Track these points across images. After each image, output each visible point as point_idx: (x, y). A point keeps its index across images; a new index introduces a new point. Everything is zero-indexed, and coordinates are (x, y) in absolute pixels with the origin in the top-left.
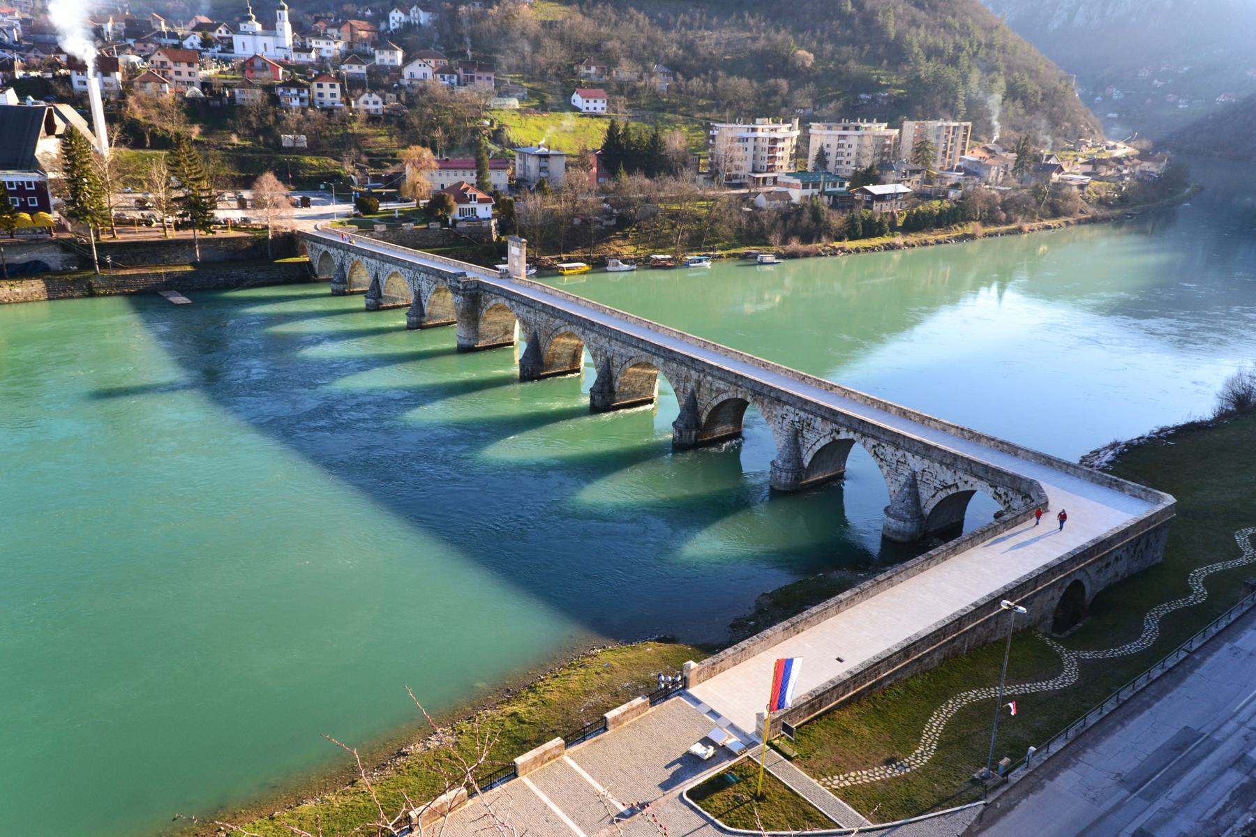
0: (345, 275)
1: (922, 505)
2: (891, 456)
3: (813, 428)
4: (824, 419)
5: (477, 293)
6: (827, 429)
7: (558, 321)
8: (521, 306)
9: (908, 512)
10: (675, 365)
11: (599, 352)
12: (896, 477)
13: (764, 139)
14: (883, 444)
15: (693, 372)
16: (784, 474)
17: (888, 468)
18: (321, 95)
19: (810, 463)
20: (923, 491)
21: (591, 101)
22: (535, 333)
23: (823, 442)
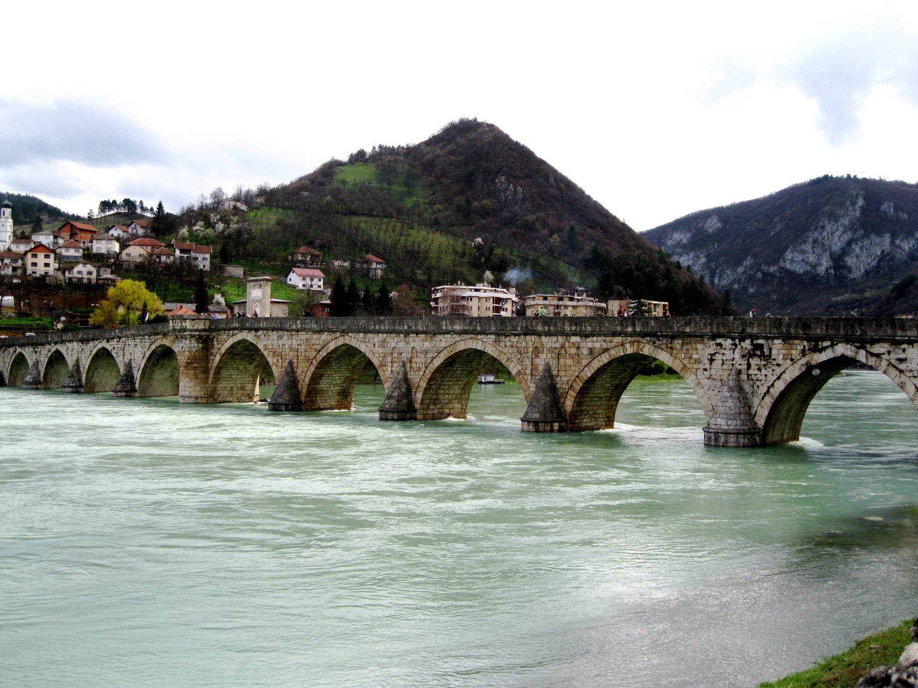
0: (39, 374)
5: (208, 336)
7: (325, 336)
8: (270, 333)
11: (389, 359)
13: (487, 299)
18: (34, 264)
19: (768, 418)
22: (291, 363)
23: (789, 377)
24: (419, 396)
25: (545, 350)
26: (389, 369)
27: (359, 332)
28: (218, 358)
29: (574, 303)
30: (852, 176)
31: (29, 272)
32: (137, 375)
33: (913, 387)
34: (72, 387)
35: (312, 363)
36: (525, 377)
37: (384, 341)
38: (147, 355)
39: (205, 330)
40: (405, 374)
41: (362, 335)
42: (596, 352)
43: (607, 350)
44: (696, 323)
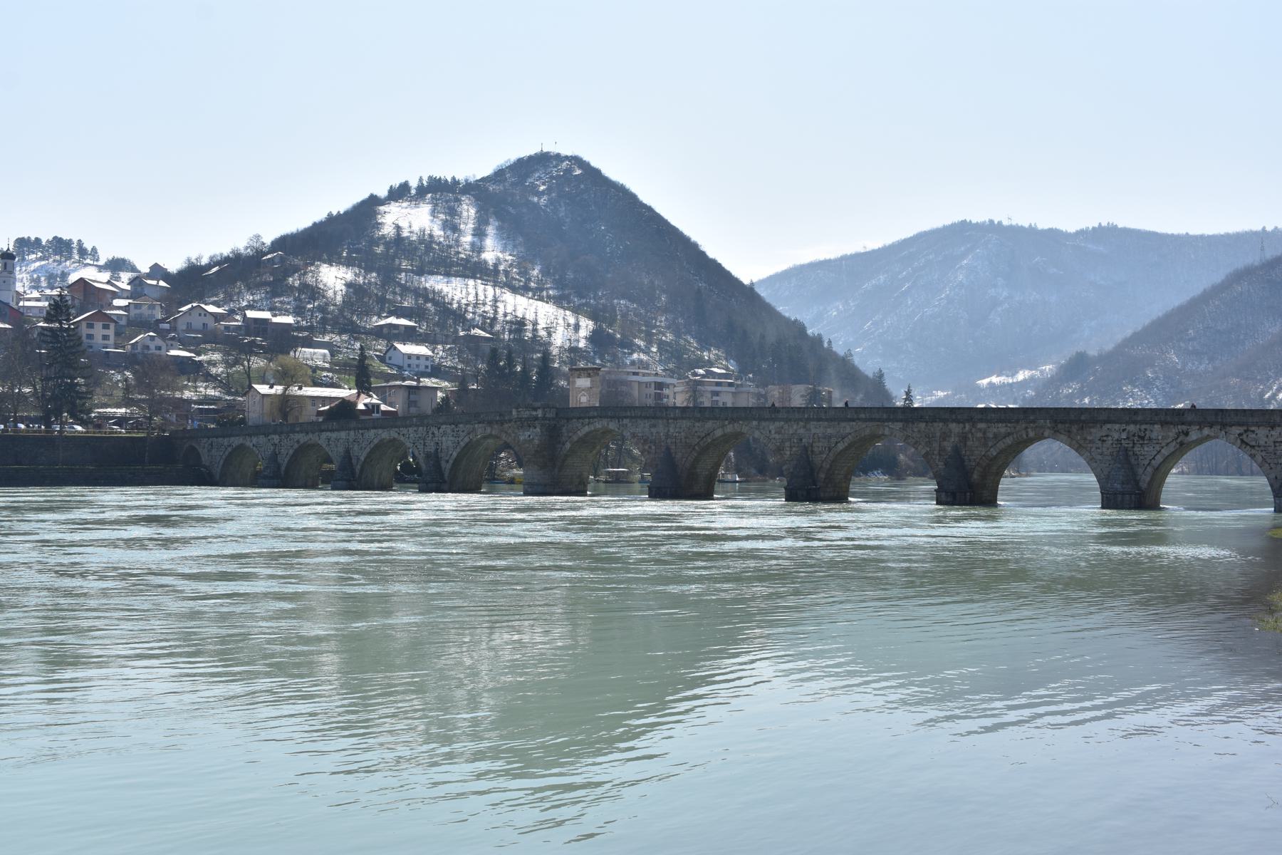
2: (1265, 439)
3: (1150, 439)
4: (1164, 424)
5: (555, 425)
6: (1170, 434)
7: (709, 424)
8: (639, 421)
10: (923, 425)
11: (787, 444)
12: (1276, 461)
13: (647, 385)
14: (1253, 428)
15: (953, 426)
16: (1127, 497)
17: (1264, 454)
18: (90, 337)
24: (822, 476)
25: (953, 435)
26: (788, 453)
28: (568, 445)
29: (733, 389)
30: (996, 222)
33: (1261, 457)
35: (694, 449)
36: (934, 457)
38: (462, 444)
39: (553, 419)
40: (808, 457)
41: (755, 423)
43: (1009, 434)
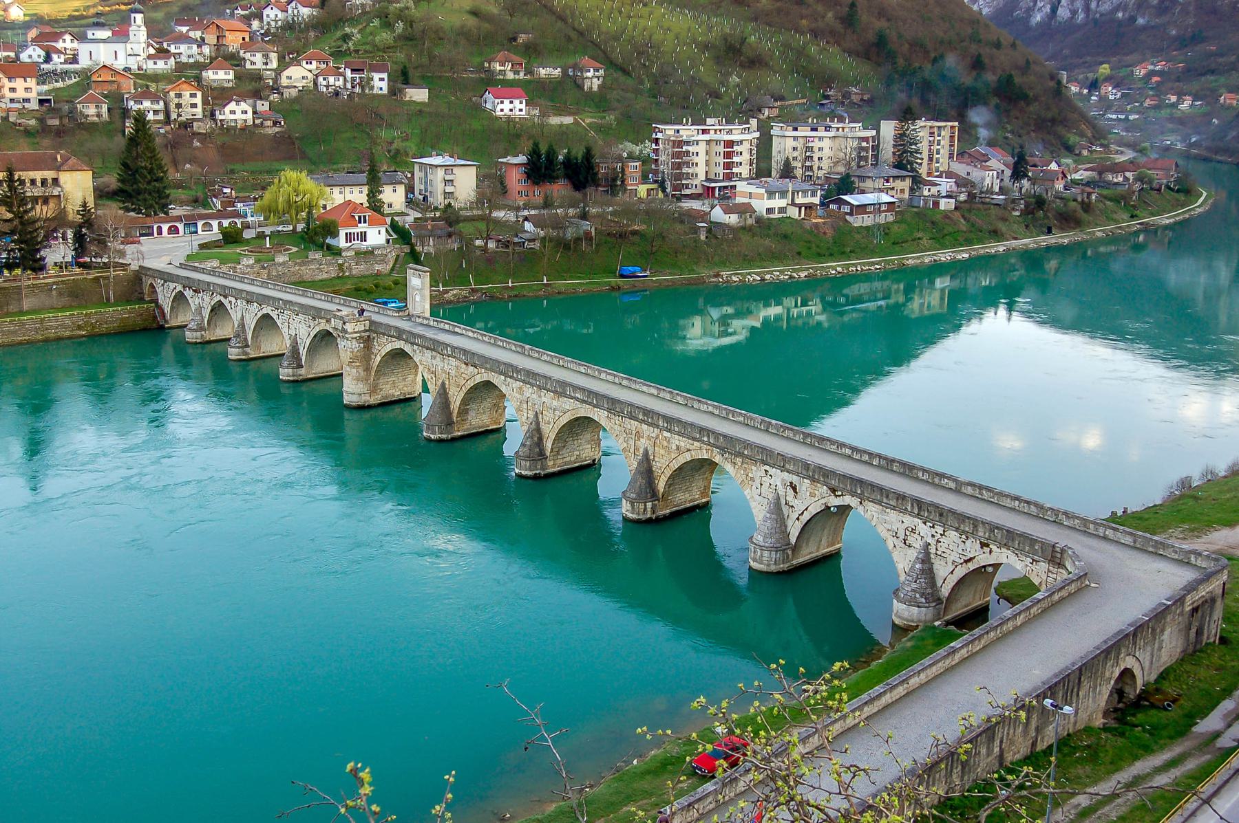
0: (203, 321)
1: (939, 585)
5: (369, 336)
9: (922, 595)
15: (645, 427)
16: (766, 554)
20: (938, 567)
21: (507, 102)
22: (443, 384)
26: (525, 414)
27: (501, 373)
28: (379, 358)
31: (174, 116)
32: (303, 353)
34: (239, 347)
37: (521, 388)
38: (312, 335)
39: (365, 331)
40: (538, 423)
41: (503, 377)
42: (683, 449)
44: (752, 449)
